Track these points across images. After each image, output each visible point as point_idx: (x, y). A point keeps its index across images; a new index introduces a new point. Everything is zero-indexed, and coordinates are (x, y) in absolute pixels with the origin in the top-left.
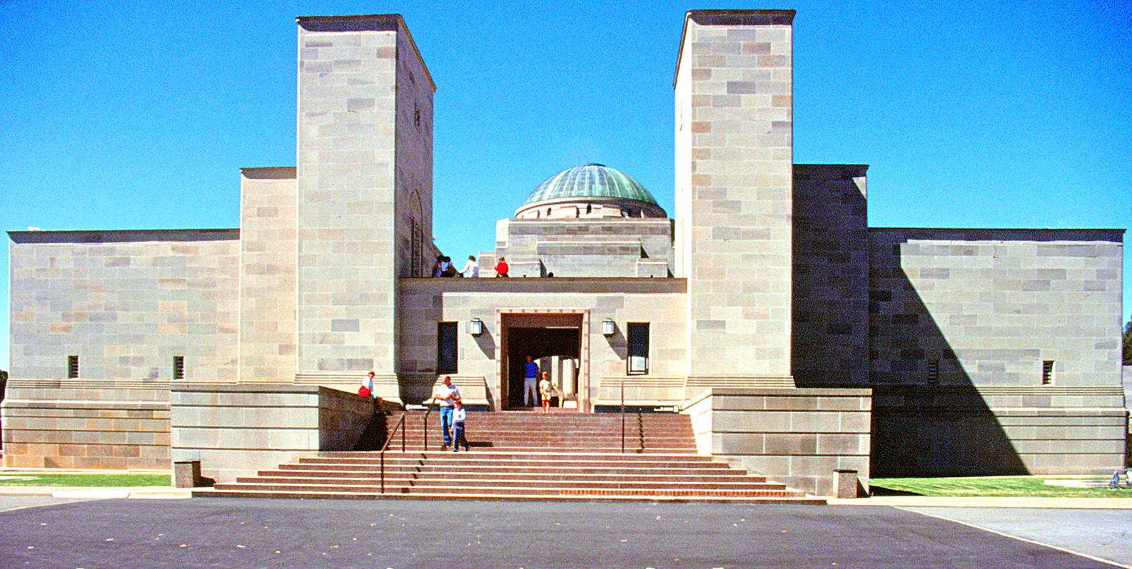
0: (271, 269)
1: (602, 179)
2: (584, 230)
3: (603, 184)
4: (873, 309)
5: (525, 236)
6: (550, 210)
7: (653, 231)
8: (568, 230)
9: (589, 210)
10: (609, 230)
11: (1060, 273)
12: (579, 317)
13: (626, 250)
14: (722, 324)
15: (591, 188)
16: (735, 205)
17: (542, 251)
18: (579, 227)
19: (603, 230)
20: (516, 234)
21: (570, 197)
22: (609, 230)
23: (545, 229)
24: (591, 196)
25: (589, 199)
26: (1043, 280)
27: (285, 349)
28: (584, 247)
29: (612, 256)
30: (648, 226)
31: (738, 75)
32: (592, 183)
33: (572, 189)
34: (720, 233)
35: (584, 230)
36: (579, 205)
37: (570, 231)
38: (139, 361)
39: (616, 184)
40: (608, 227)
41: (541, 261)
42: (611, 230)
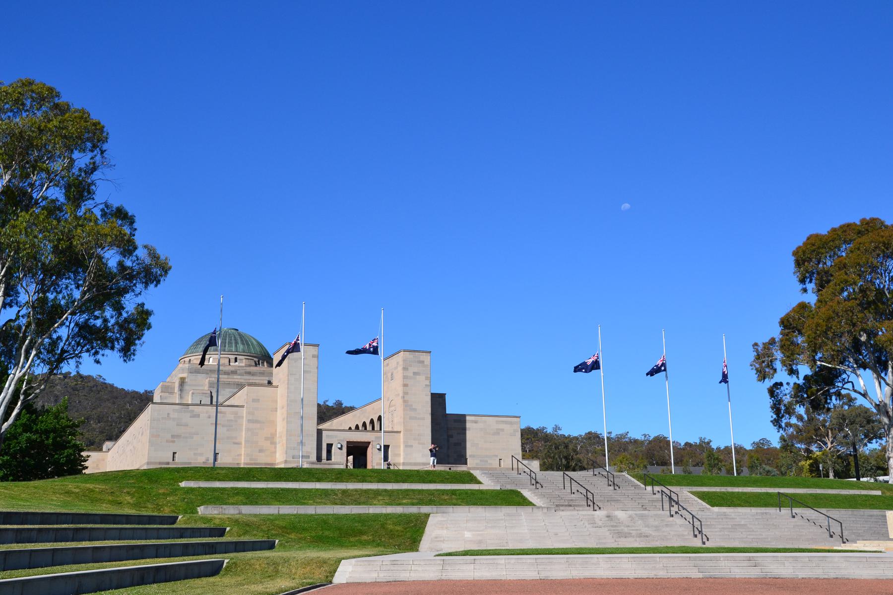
0: (257, 422)
1: (242, 340)
2: (234, 372)
3: (243, 344)
4: (448, 441)
9: (236, 360)
10: (249, 373)
11: (502, 430)
12: (369, 443)
14: (411, 446)
15: (236, 346)
16: (415, 410)
22: (249, 373)
26: (498, 432)
27: (261, 451)
31: (416, 371)
32: (236, 343)
34: (411, 418)
35: (234, 372)
38: (201, 454)
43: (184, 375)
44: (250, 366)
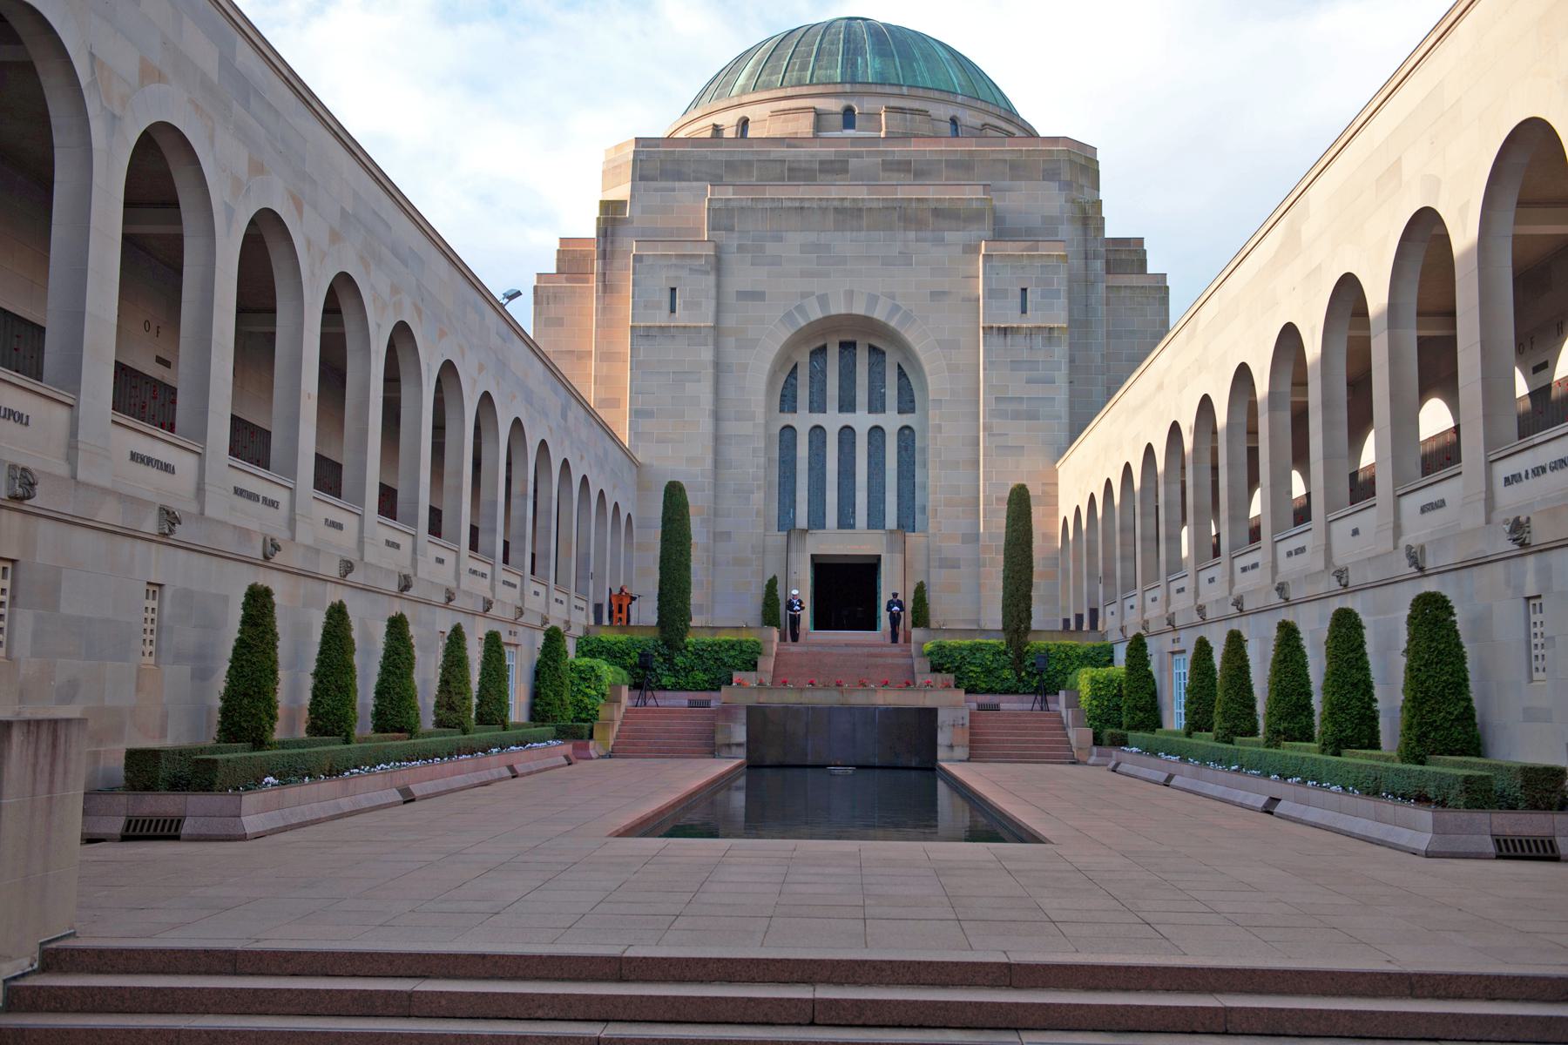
2: (835, 168)
5: (677, 184)
6: (744, 123)
7: (1016, 169)
8: (790, 170)
10: (903, 166)
13: (946, 215)
17: (722, 217)
18: (821, 162)
19: (884, 170)
20: (654, 179)
21: (800, 84)
23: (731, 166)
24: (853, 82)
25: (848, 88)
28: (836, 209)
29: (912, 235)
30: (1008, 157)
33: (803, 68)
35: (835, 168)
36: (820, 104)
37: (796, 173)
39: (918, 55)
40: (899, 162)
41: (719, 248)
42: (909, 171)
43: (622, 192)
44: (906, 137)
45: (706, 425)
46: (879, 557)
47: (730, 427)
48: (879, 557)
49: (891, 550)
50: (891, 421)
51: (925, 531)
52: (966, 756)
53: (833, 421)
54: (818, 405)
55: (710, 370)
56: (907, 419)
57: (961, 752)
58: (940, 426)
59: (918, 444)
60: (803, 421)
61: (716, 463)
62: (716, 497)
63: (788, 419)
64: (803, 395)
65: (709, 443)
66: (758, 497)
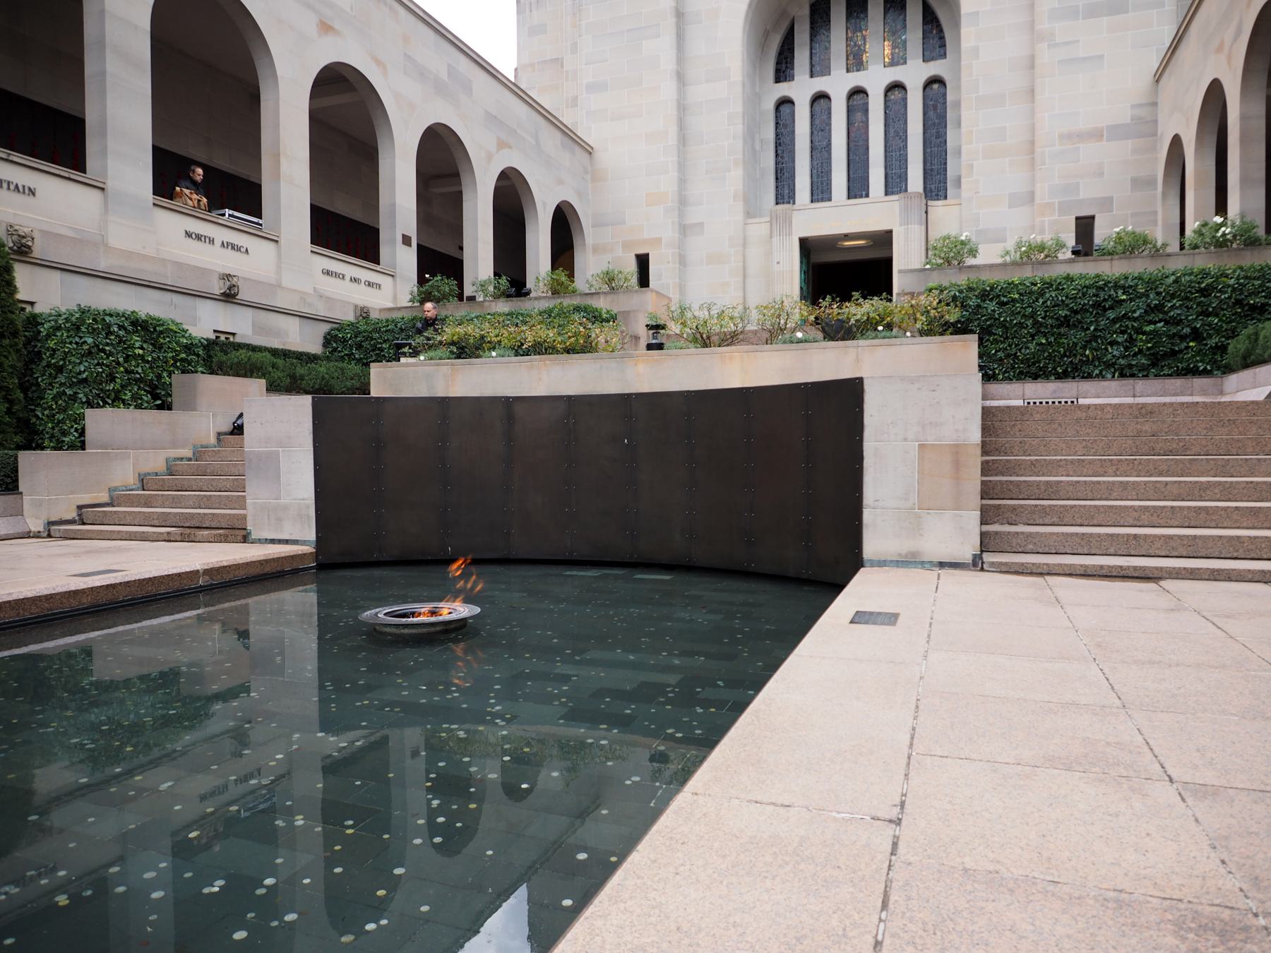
45: (669, 89)
46: (890, 232)
47: (699, 92)
48: (890, 232)
49: (905, 222)
50: (914, 73)
51: (959, 196)
52: (967, 548)
53: (838, 84)
54: (818, 68)
55: (671, 20)
56: (935, 68)
57: (957, 532)
58: (976, 50)
59: (949, 98)
60: (801, 89)
61: (683, 140)
62: (683, 181)
63: (784, 89)
64: (801, 57)
65: (672, 110)
66: (736, 178)
